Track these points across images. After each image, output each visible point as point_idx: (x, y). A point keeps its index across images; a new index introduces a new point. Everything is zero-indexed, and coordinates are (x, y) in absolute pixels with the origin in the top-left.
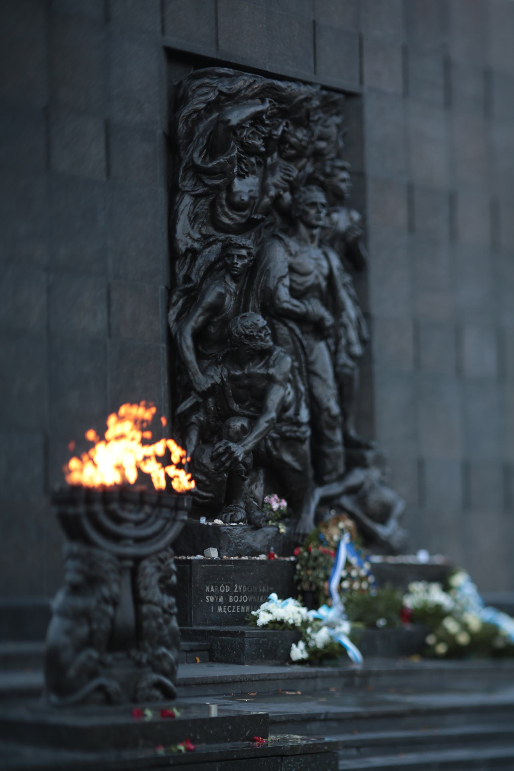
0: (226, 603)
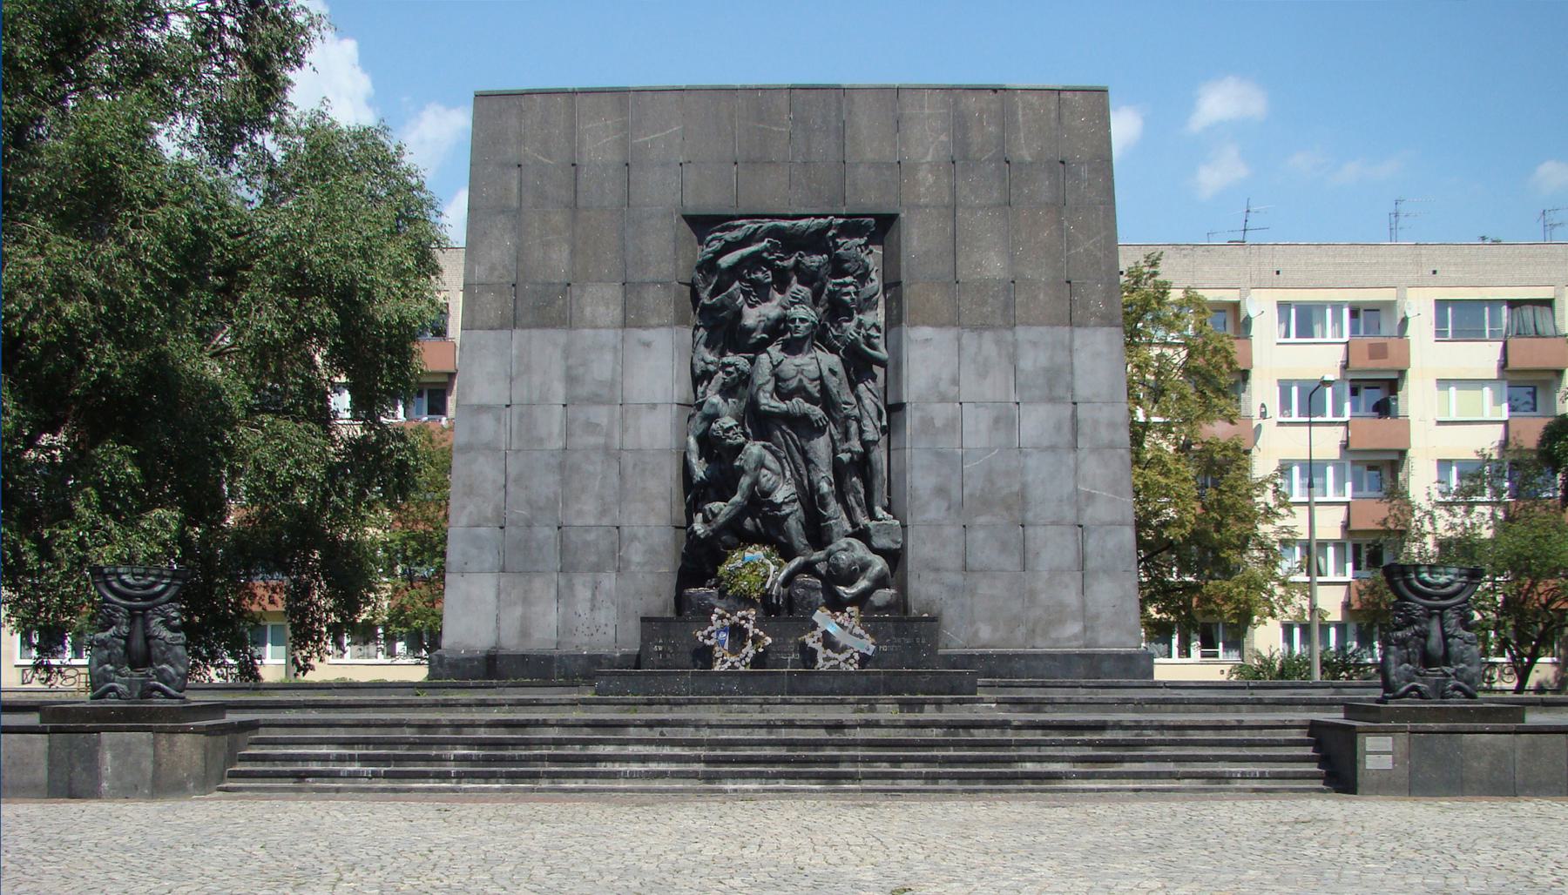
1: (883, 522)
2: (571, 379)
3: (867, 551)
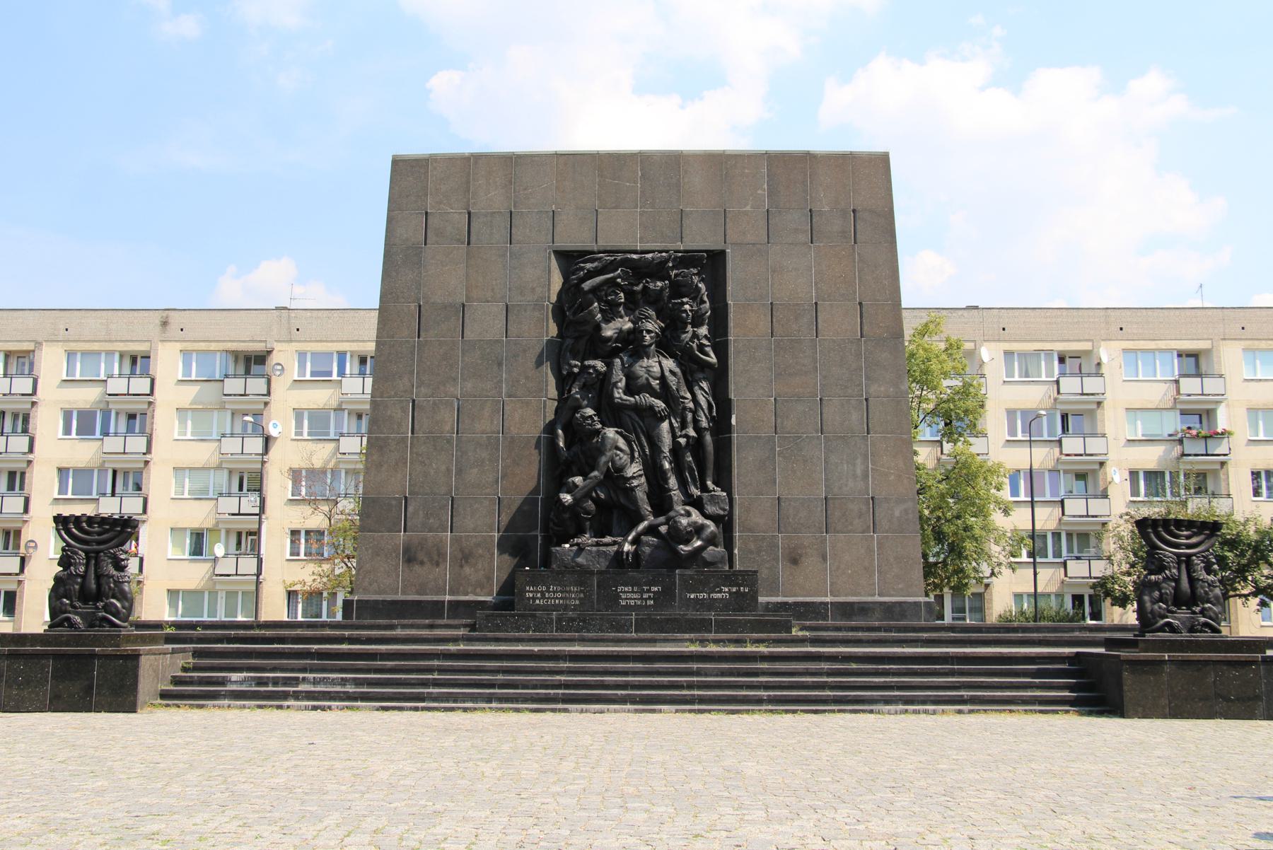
0: (543, 597)
1: (713, 493)
3: (701, 517)
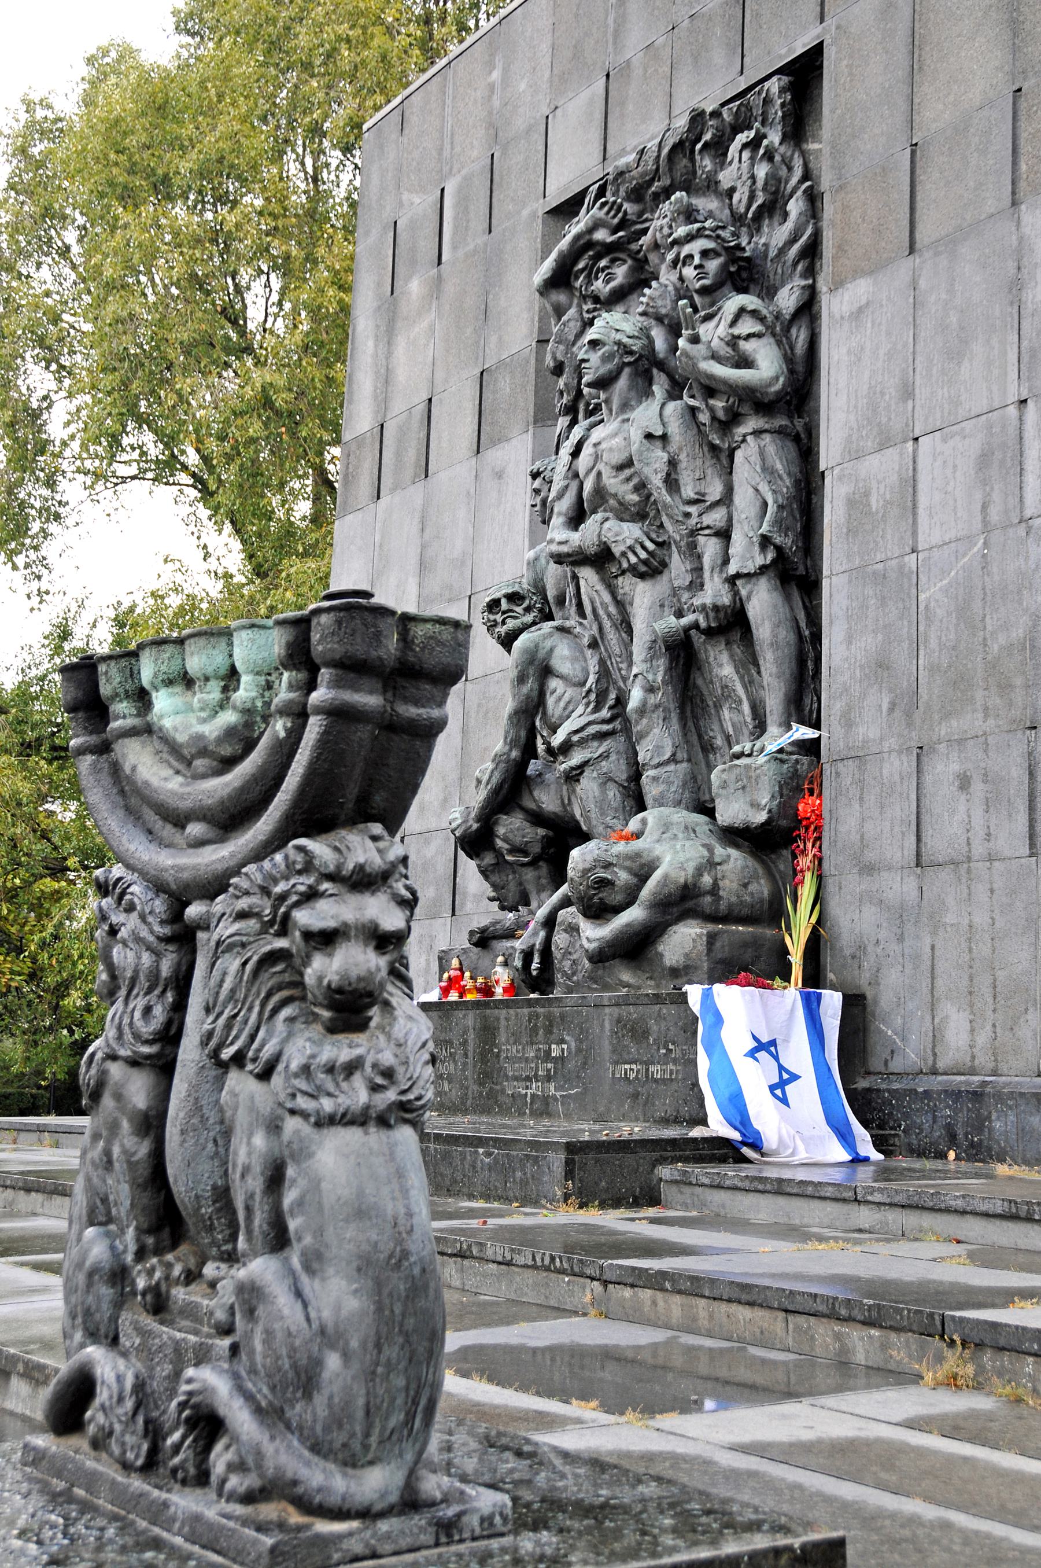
2: (424, 567)
